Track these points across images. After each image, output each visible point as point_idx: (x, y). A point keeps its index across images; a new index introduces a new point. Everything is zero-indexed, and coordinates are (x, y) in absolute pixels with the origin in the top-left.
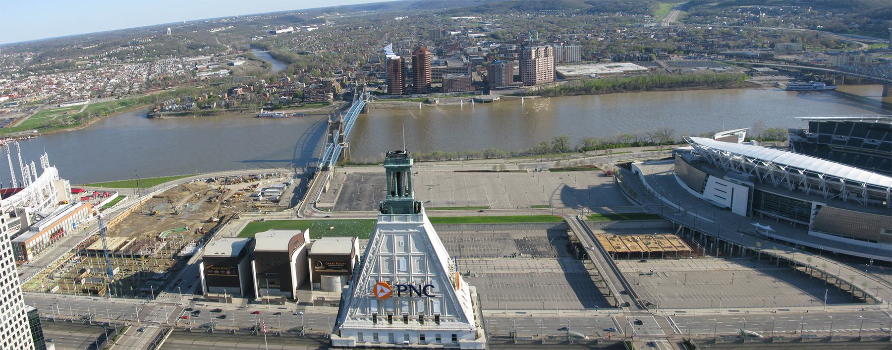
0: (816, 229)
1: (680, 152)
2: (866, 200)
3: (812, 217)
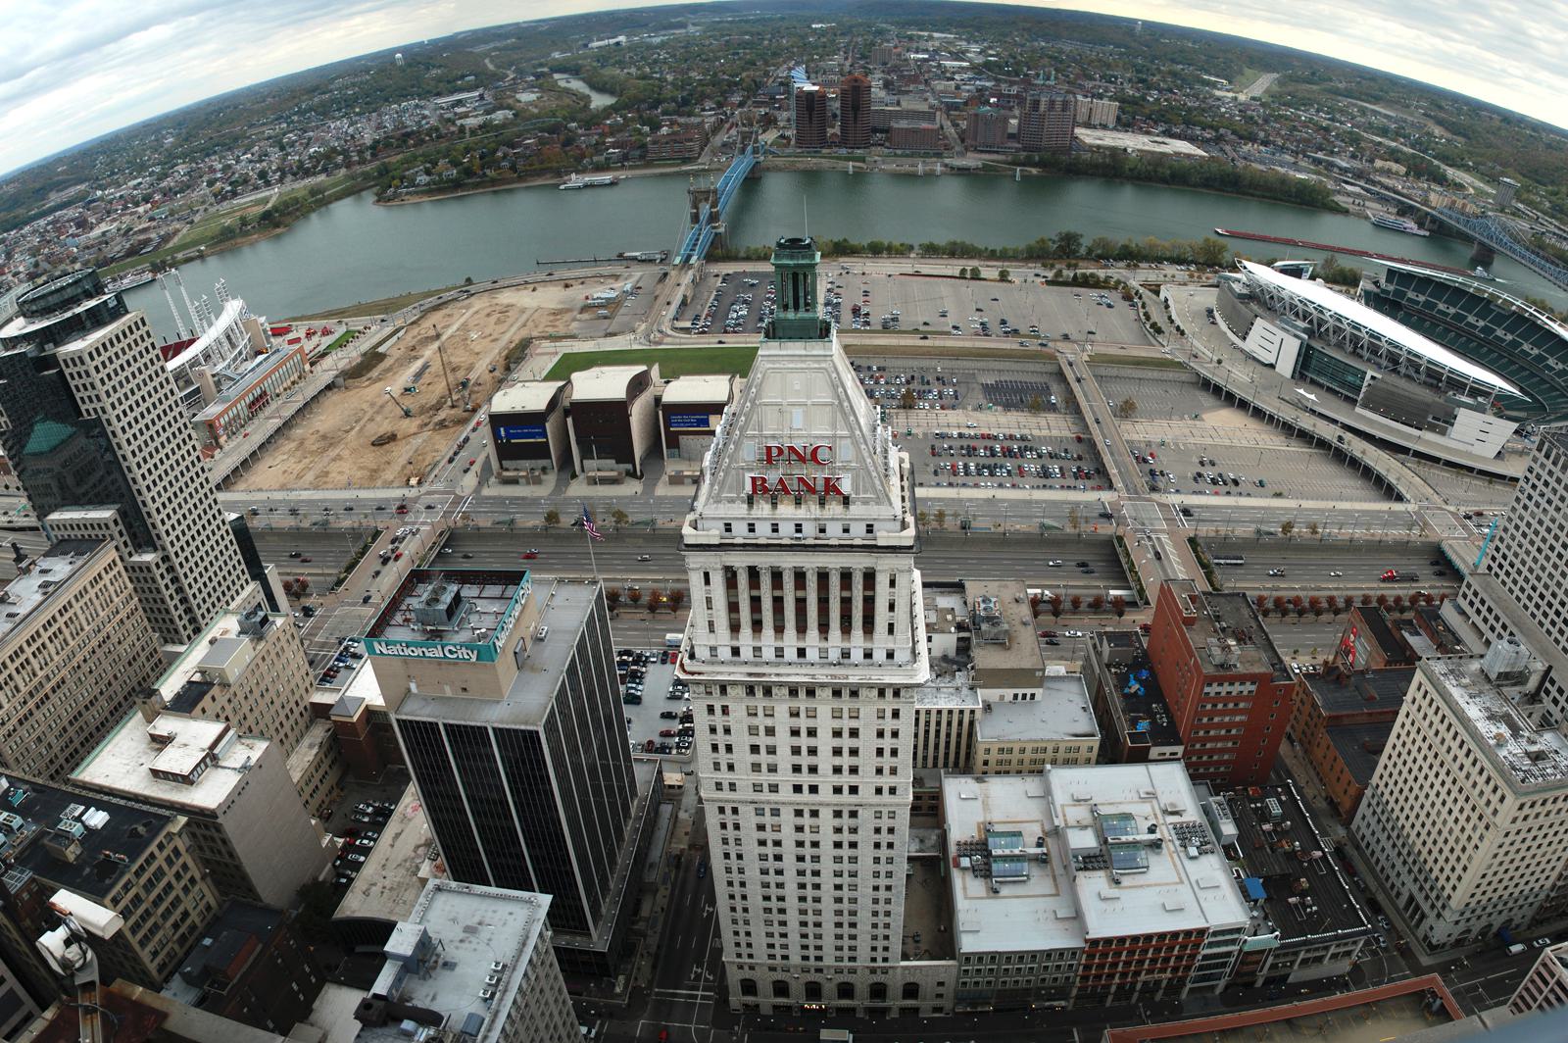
0: (1365, 406)
1: (1228, 279)
2: (1423, 377)
3: (1364, 390)
